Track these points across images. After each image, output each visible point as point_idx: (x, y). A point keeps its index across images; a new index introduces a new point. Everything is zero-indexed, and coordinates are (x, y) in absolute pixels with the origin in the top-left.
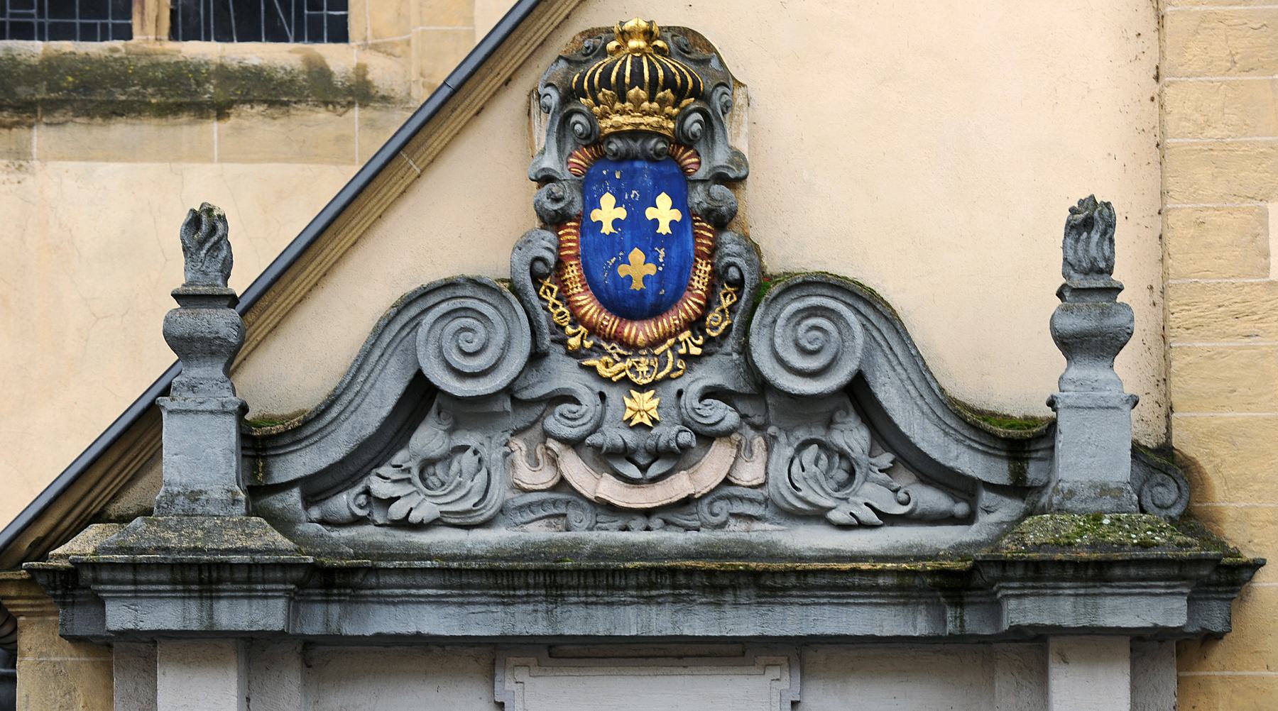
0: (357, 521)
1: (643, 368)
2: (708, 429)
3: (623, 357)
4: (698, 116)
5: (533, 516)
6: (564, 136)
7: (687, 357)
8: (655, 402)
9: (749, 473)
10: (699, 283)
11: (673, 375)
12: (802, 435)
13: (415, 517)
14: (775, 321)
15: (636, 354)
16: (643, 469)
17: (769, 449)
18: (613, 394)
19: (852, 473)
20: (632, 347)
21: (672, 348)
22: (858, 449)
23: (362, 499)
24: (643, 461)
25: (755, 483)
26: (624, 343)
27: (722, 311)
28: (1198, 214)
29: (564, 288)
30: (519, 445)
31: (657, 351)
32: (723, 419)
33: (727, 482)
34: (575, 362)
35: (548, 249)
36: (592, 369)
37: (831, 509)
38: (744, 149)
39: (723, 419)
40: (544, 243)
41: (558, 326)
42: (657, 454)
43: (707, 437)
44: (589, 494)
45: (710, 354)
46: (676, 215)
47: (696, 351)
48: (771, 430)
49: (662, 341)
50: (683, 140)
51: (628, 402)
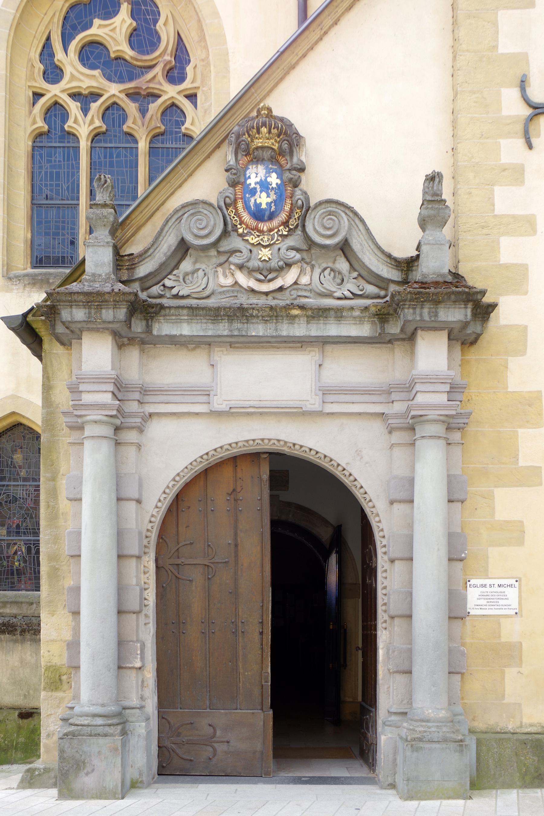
0: (161, 296)
1: (266, 239)
2: (290, 260)
3: (258, 236)
4: (286, 142)
5: (225, 296)
6: (237, 153)
7: (282, 236)
8: (271, 252)
9: (305, 280)
10: (287, 208)
11: (277, 243)
12: (324, 265)
13: (181, 294)
14: (315, 218)
15: (263, 235)
16: (266, 277)
17: (312, 271)
18: (254, 250)
19: (343, 280)
20: (262, 232)
21: (276, 233)
22: (344, 270)
23: (162, 287)
24: (265, 274)
25: (307, 283)
26: (259, 231)
27: (295, 219)
28: (469, 190)
29: (236, 209)
30: (220, 270)
31: (272, 233)
32: (295, 256)
33: (296, 283)
34: (241, 238)
35: (231, 193)
36: (247, 240)
37: (335, 292)
38: (304, 161)
39: (295, 256)
40: (230, 192)
41: (235, 225)
42: (270, 271)
43: (289, 265)
44: (245, 286)
45: (291, 235)
46: (279, 181)
47: (286, 233)
48: (313, 262)
49: (273, 230)
50: (281, 153)
51: (260, 252)
